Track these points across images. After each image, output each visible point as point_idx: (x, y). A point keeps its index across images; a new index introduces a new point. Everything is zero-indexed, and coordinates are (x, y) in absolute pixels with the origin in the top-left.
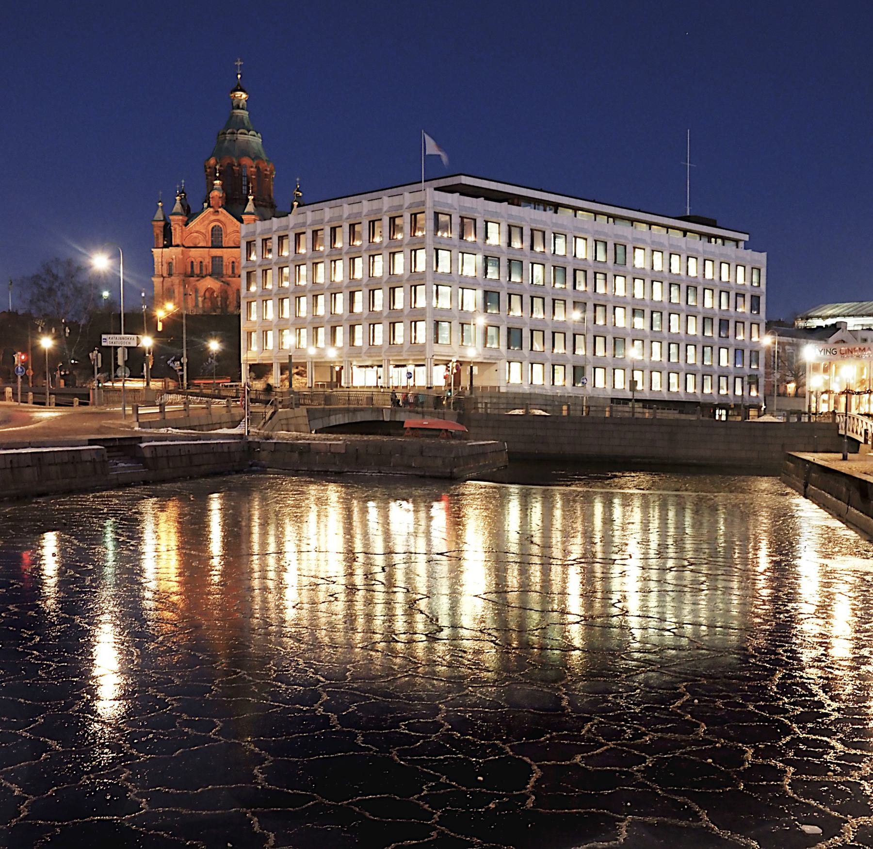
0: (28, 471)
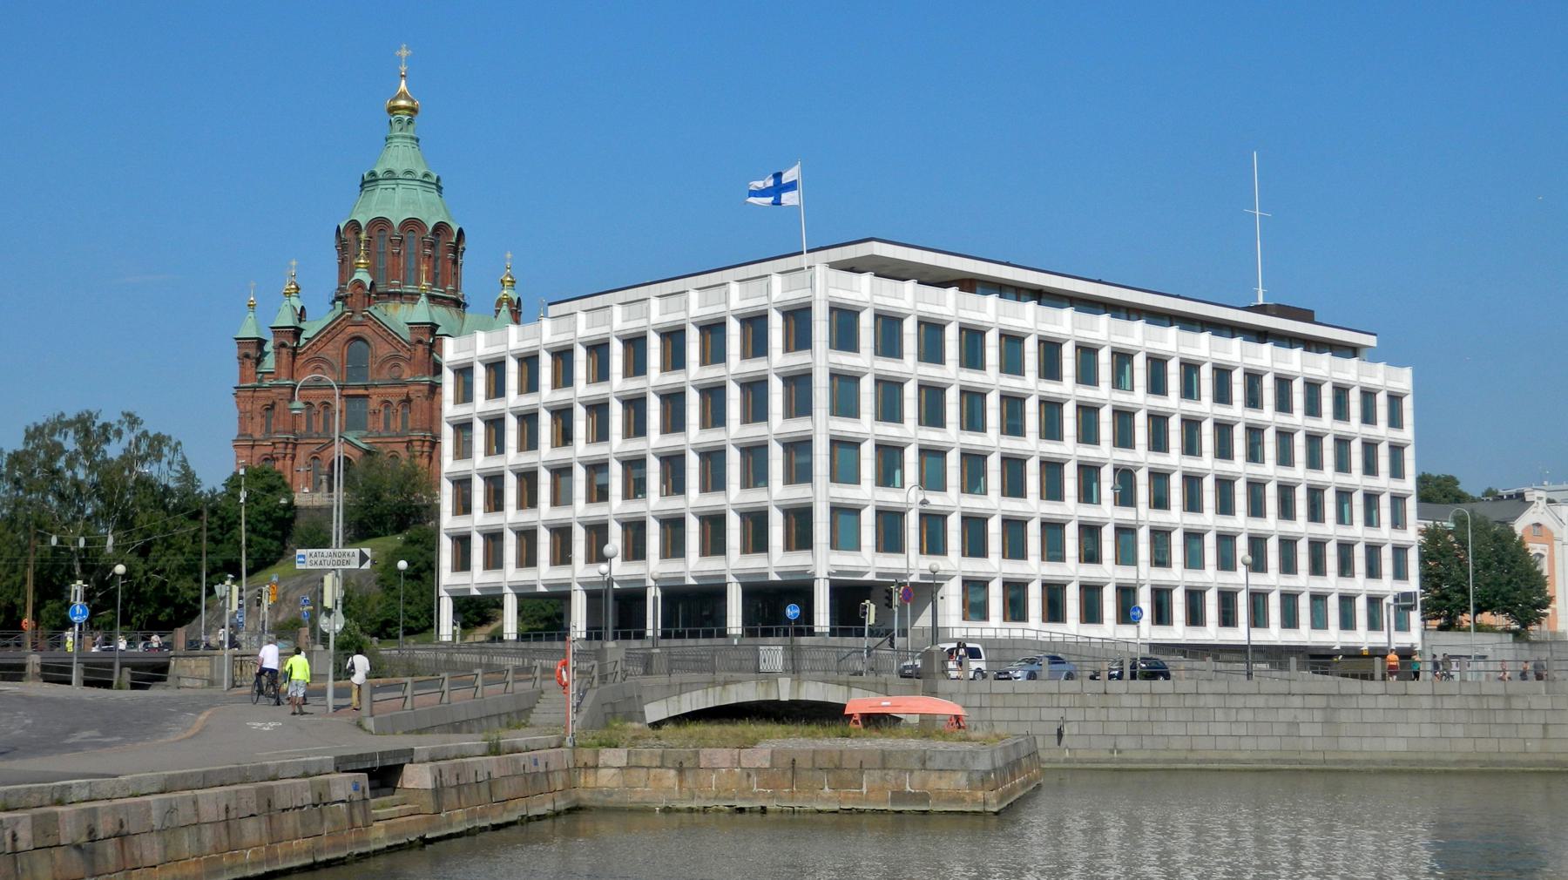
0: (251, 823)
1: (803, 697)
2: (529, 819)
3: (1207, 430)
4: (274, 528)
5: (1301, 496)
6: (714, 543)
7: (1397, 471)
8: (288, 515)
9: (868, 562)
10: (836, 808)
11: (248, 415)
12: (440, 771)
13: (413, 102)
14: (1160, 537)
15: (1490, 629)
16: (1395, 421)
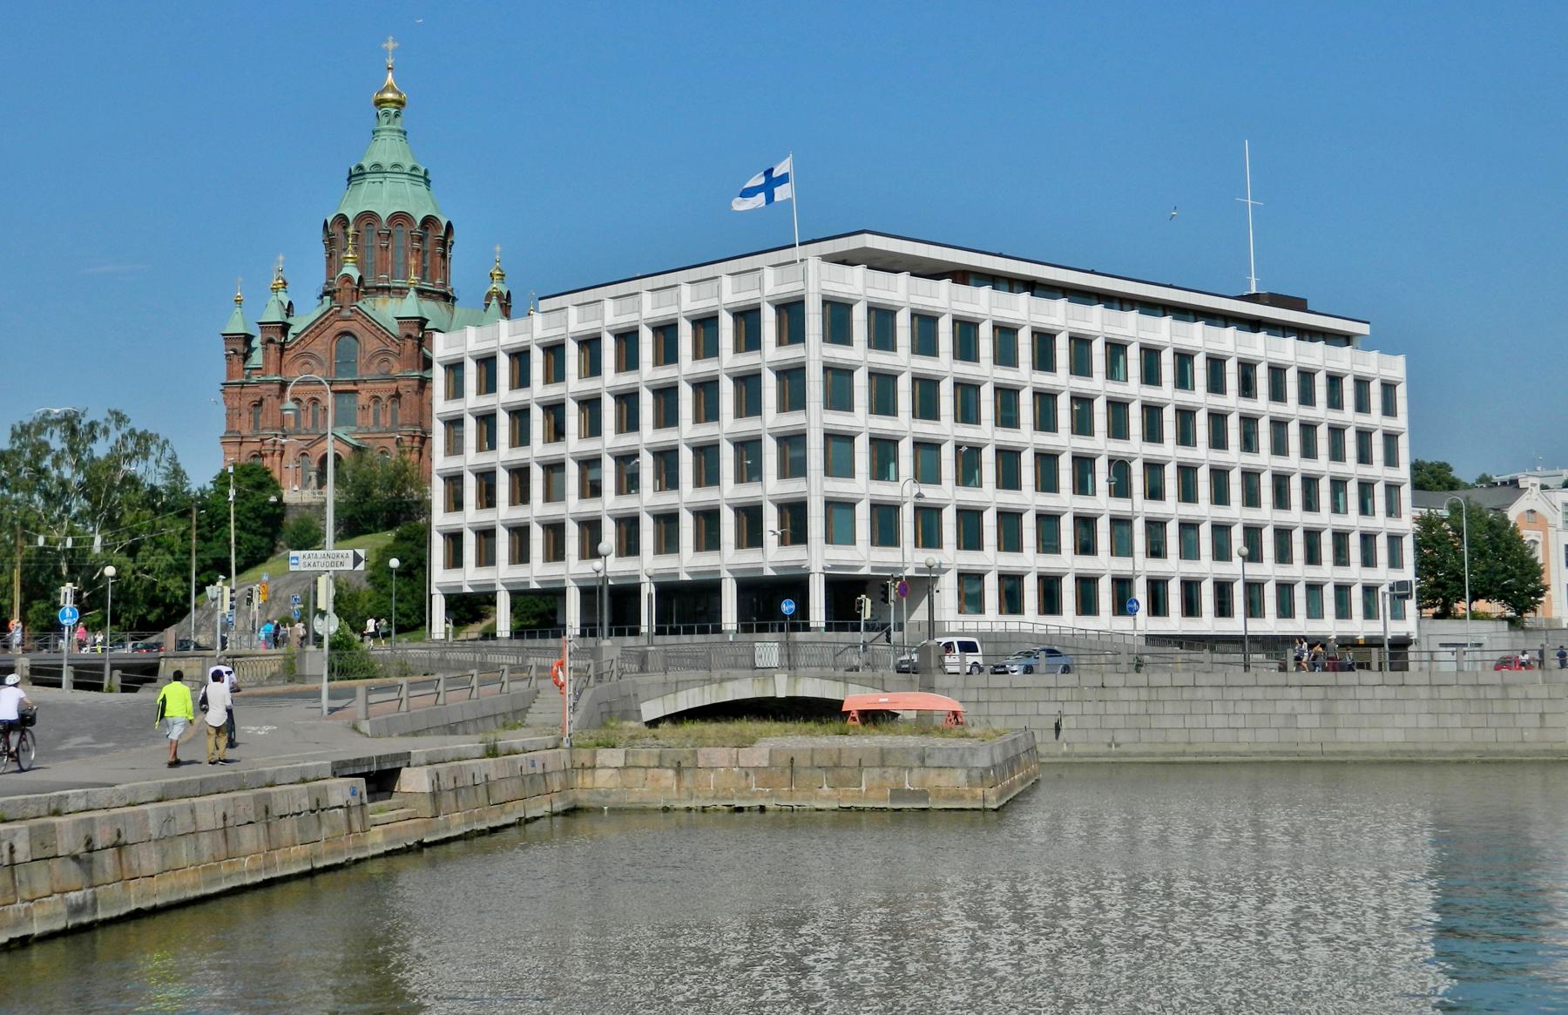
0: (248, 832)
1: (800, 694)
2: (528, 821)
3: (1202, 421)
4: (264, 525)
5: (1296, 486)
6: (708, 536)
7: (1391, 460)
8: (278, 511)
9: (863, 556)
10: (836, 806)
11: (236, 411)
12: (438, 775)
13: (400, 94)
14: (1155, 527)
15: (1486, 617)
16: (1389, 409)
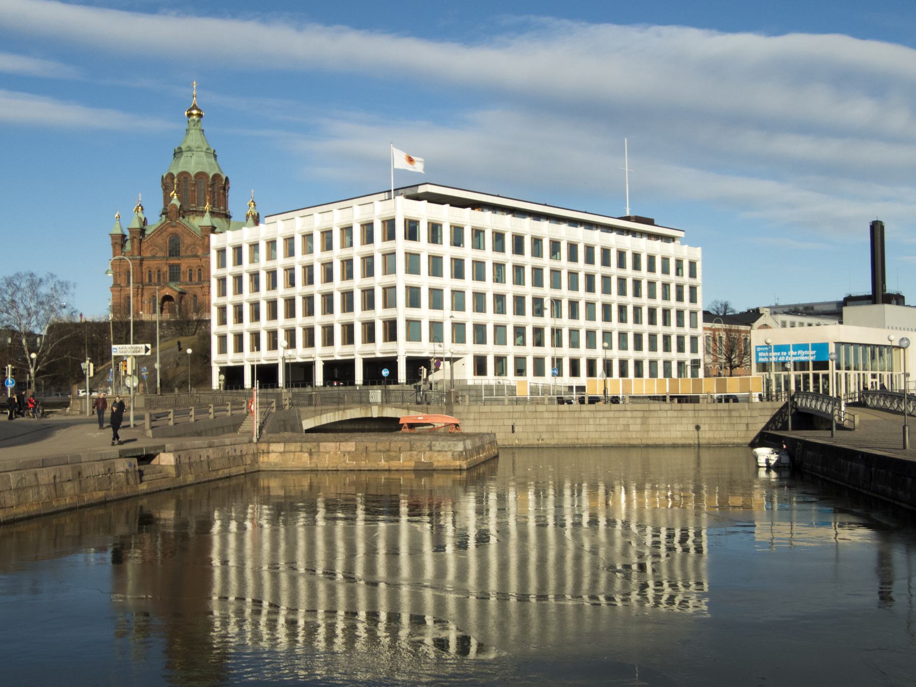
1: (385, 415)
6: (349, 338)
9: (424, 348)
16: (693, 274)
